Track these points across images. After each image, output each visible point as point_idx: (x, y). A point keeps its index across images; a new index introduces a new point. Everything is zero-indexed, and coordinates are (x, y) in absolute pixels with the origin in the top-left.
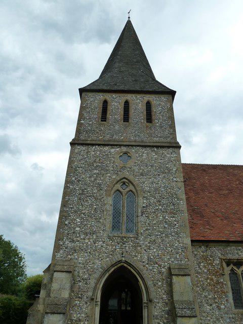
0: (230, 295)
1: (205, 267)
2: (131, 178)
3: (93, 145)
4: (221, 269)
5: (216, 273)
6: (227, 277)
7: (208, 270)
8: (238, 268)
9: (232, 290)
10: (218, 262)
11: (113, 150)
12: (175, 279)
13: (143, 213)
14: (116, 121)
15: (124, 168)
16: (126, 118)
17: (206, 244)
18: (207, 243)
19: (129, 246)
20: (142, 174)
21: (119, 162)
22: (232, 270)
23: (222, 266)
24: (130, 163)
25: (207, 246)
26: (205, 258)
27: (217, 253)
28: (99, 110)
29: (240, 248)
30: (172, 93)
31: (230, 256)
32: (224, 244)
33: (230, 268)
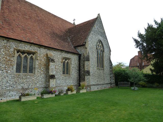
1: (4, 51)
4: (14, 54)
5: (10, 56)
6: (15, 58)
7: (5, 53)
8: (23, 55)
9: (17, 64)
10: (12, 50)
17: (7, 40)
22: (19, 55)
23: (14, 52)
25: (8, 41)
26: (5, 47)
27: (13, 45)
29: (27, 45)
31: (20, 48)
32: (18, 42)
33: (18, 54)
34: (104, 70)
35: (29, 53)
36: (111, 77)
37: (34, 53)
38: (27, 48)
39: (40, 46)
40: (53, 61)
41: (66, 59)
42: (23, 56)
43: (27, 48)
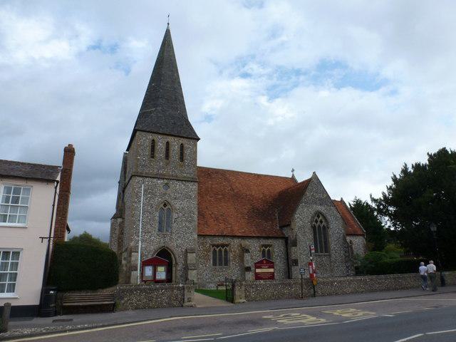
0: (212, 260)
2: (169, 200)
3: (146, 177)
11: (159, 182)
12: (189, 254)
13: (175, 222)
14: (161, 159)
15: (165, 194)
16: (167, 156)
18: (204, 236)
19: (167, 239)
20: (175, 199)
21: (163, 190)
24: (169, 191)
27: (209, 241)
28: (149, 149)
30: (198, 139)
31: (215, 243)
34: (330, 256)
35: (223, 246)
36: (347, 267)
37: (227, 245)
38: (221, 241)
39: (234, 237)
40: (247, 251)
41: (266, 246)
42: (217, 250)
43: (221, 241)
